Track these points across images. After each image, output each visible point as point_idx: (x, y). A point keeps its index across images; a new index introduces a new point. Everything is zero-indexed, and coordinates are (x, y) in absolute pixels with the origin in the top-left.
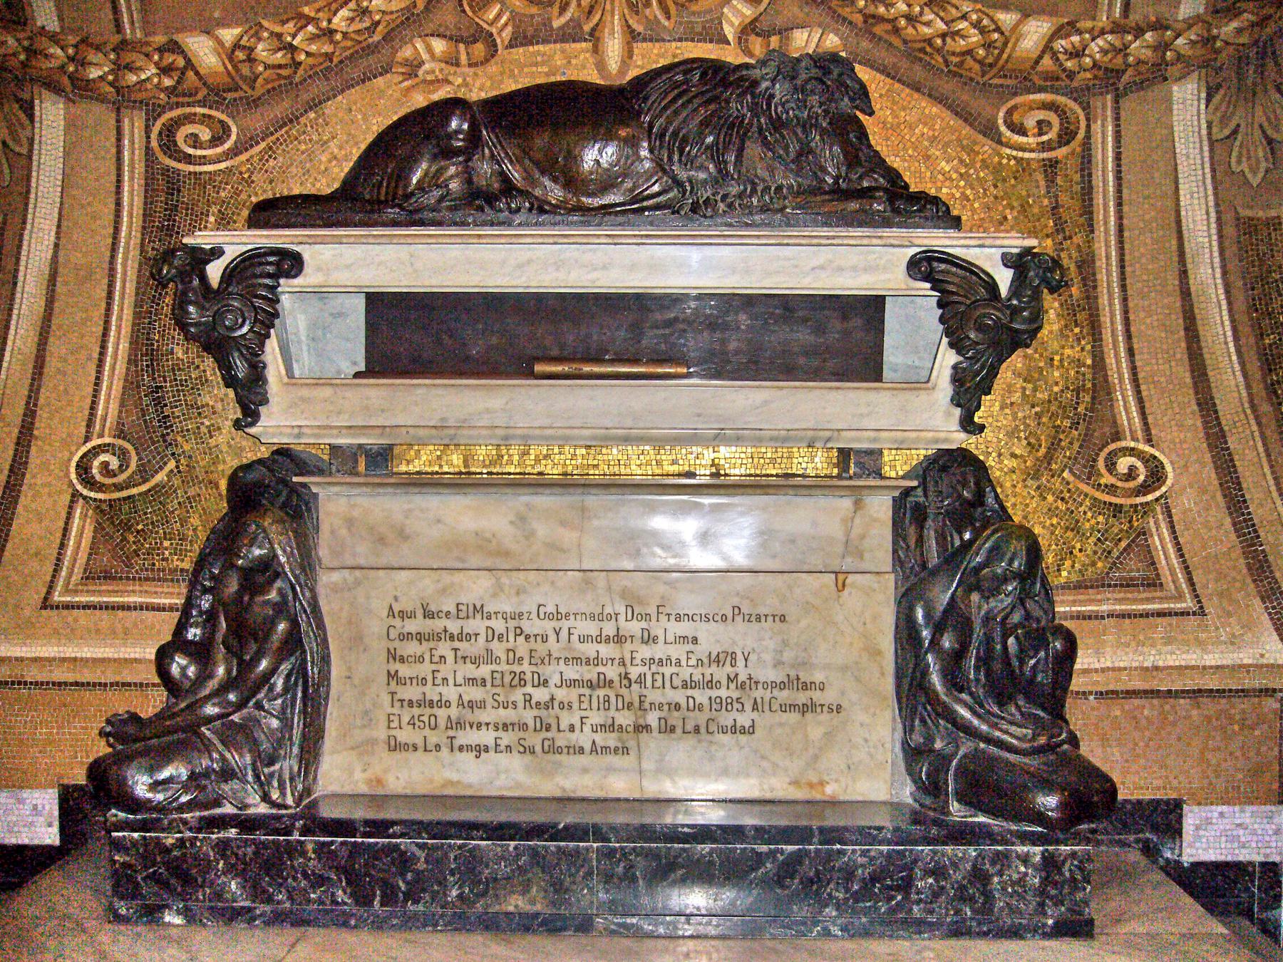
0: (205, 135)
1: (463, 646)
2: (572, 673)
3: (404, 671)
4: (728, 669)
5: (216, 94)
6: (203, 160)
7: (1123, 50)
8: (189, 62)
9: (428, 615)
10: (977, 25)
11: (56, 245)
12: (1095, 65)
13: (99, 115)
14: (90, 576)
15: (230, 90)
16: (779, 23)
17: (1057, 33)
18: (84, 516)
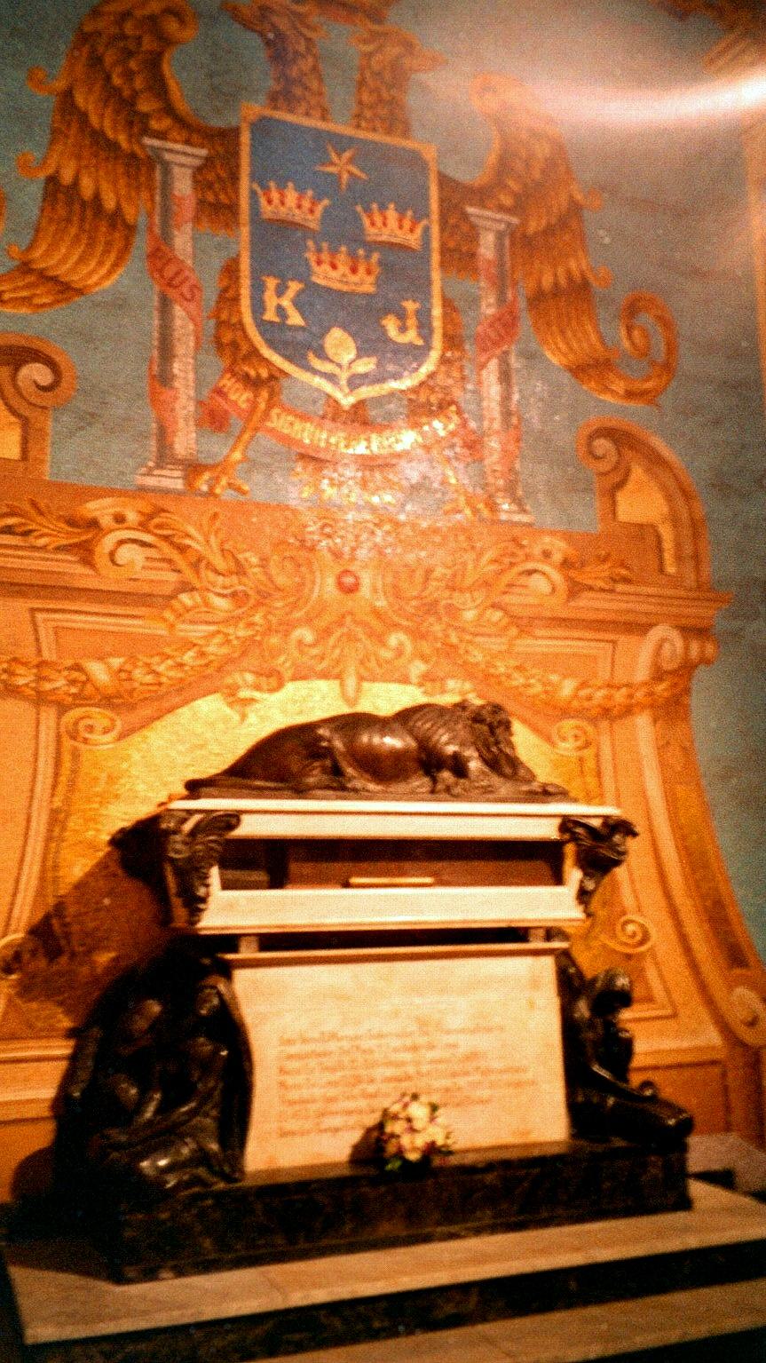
2: (389, 1072)
15: (117, 697)
16: (441, 674)
17: (578, 689)
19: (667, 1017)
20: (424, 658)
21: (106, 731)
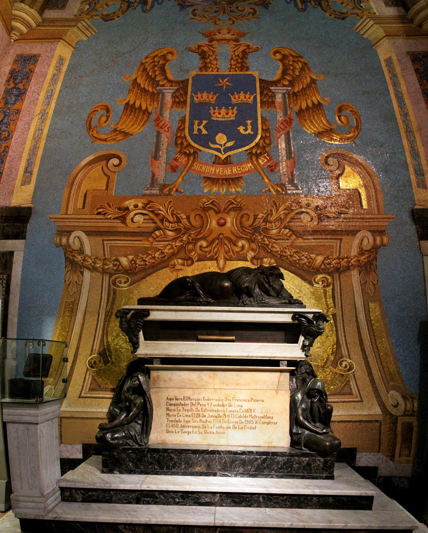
0: (123, 281)
1: (185, 407)
2: (212, 414)
3: (171, 413)
4: (250, 413)
5: (126, 271)
6: (122, 287)
8: (120, 264)
9: (177, 399)
10: (306, 257)
11: (86, 307)
12: (334, 267)
13: (98, 275)
14: (91, 390)
16: (261, 257)
17: (325, 259)
18: (90, 374)
19: (358, 401)
20: (253, 250)
21: (125, 283)
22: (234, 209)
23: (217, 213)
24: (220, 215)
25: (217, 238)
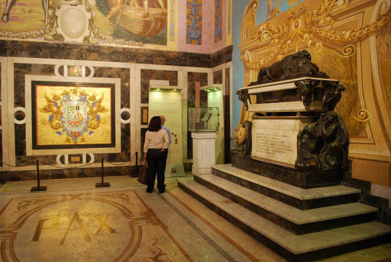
2: (270, 143)
7: (361, 33)
17: (351, 33)
20: (311, 39)
22: (303, 13)
23: (294, 19)
24: (296, 20)
25: (295, 36)
